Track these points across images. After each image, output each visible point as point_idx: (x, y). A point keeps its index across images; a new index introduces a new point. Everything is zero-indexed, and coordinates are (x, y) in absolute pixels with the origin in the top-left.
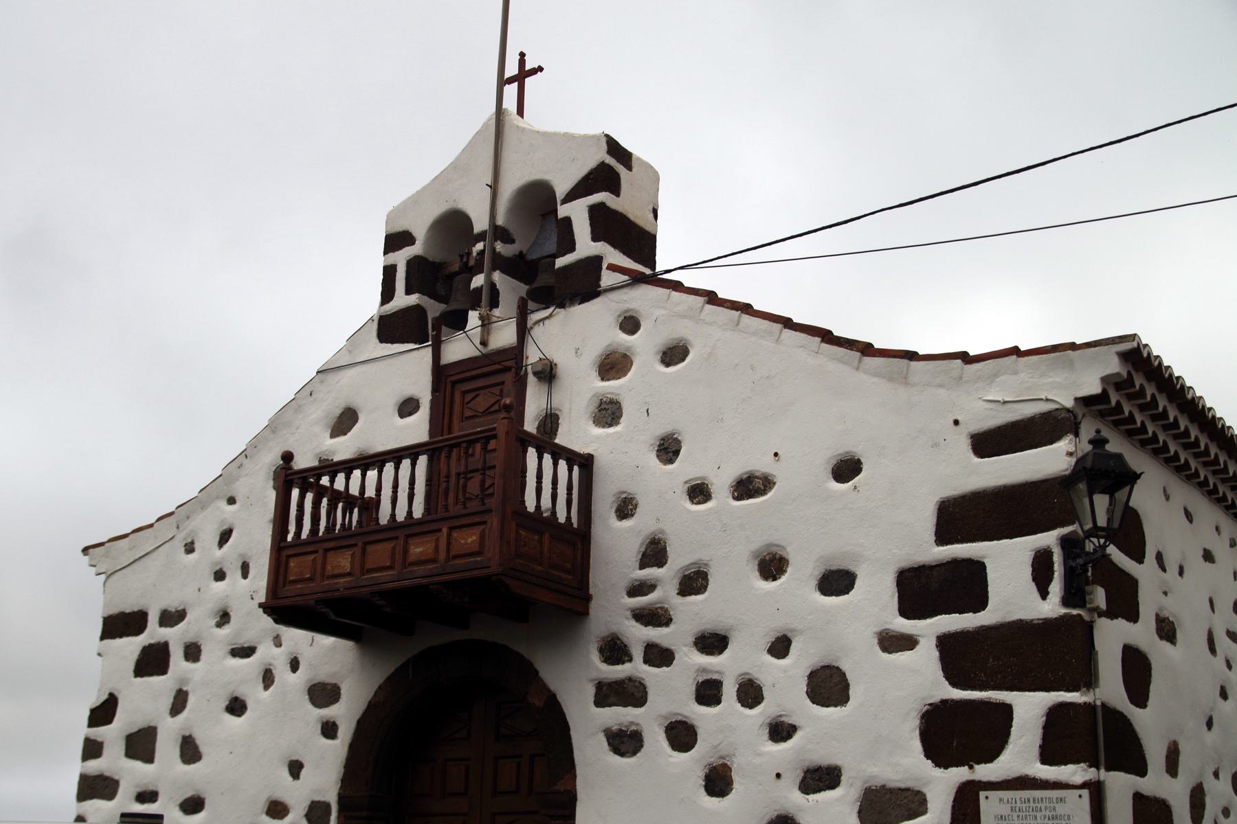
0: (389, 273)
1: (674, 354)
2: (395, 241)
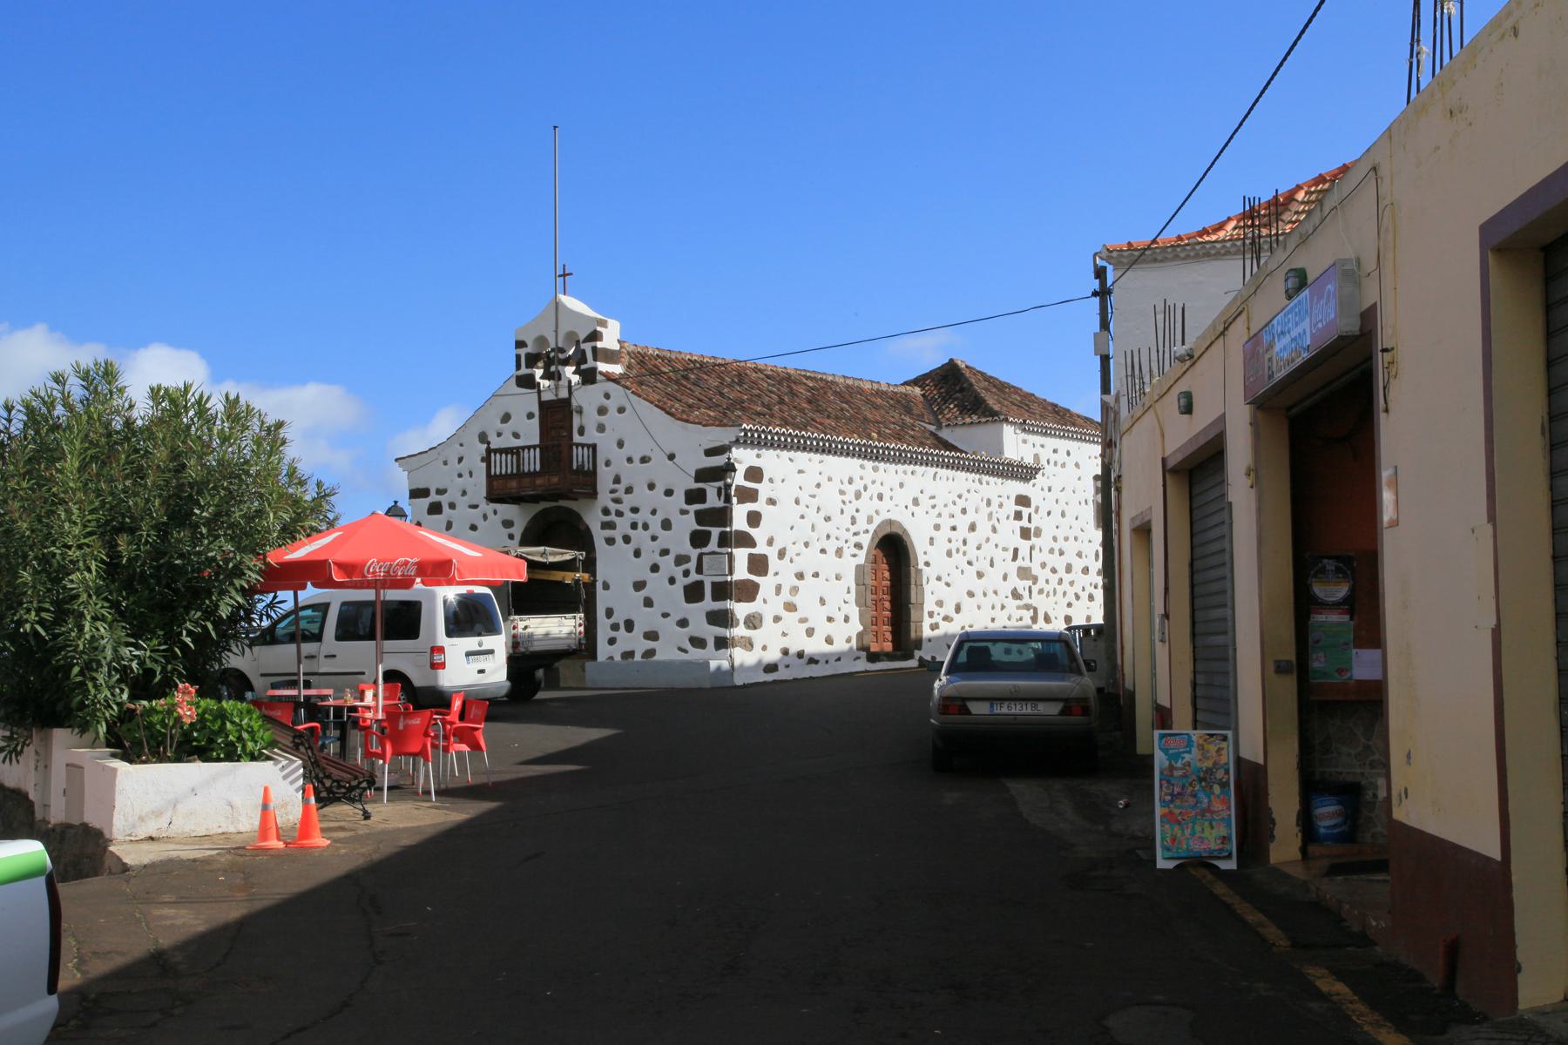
0: (518, 357)
1: (621, 410)
2: (520, 344)
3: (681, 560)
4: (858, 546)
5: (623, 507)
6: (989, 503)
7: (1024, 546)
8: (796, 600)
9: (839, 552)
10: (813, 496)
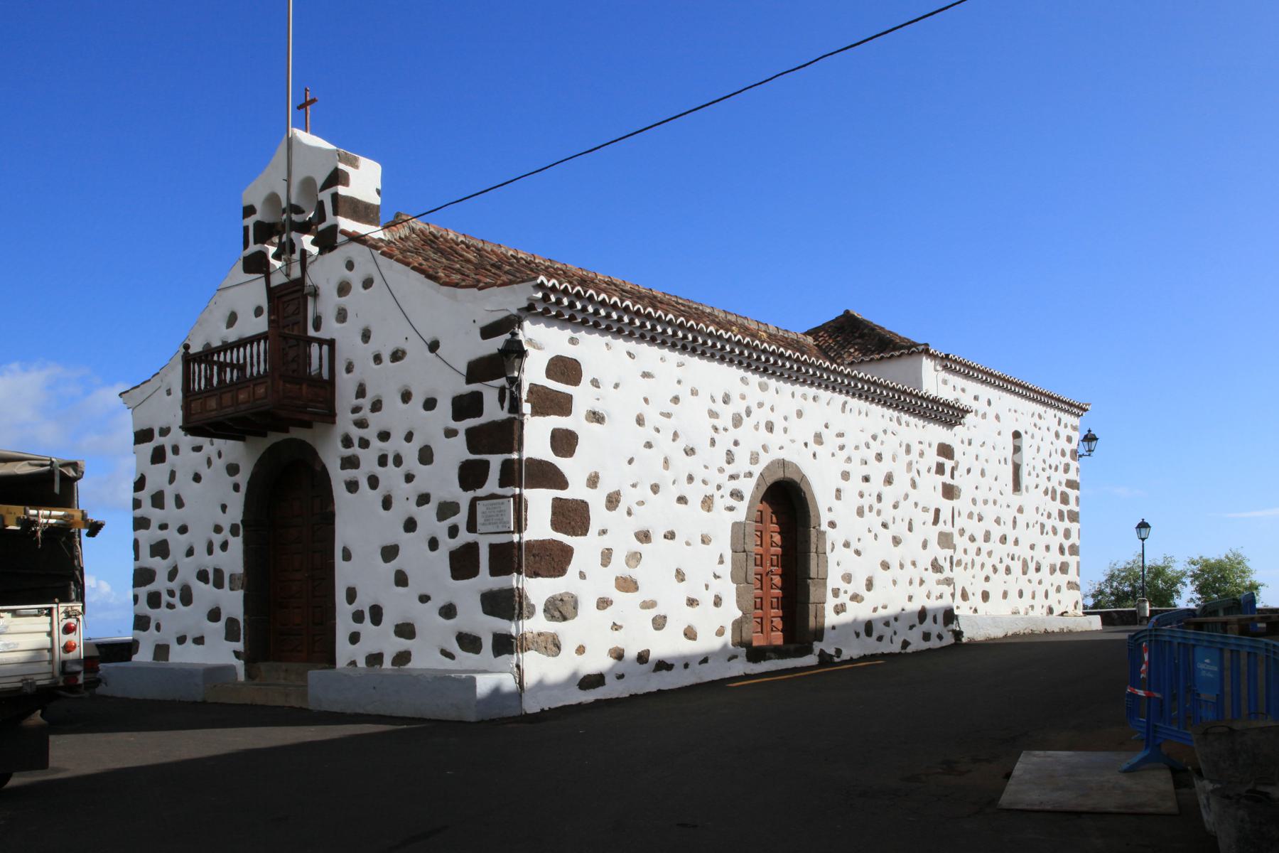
0: (246, 229)
3: (447, 510)
4: (737, 495)
5: (371, 433)
6: (908, 451)
7: (946, 506)
8: (637, 573)
9: (707, 503)
10: (668, 415)
